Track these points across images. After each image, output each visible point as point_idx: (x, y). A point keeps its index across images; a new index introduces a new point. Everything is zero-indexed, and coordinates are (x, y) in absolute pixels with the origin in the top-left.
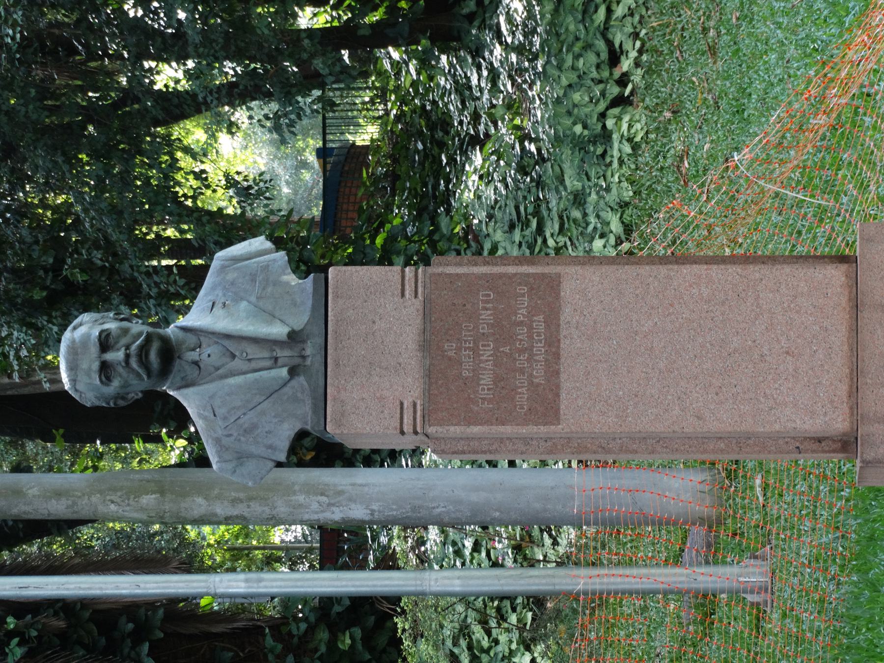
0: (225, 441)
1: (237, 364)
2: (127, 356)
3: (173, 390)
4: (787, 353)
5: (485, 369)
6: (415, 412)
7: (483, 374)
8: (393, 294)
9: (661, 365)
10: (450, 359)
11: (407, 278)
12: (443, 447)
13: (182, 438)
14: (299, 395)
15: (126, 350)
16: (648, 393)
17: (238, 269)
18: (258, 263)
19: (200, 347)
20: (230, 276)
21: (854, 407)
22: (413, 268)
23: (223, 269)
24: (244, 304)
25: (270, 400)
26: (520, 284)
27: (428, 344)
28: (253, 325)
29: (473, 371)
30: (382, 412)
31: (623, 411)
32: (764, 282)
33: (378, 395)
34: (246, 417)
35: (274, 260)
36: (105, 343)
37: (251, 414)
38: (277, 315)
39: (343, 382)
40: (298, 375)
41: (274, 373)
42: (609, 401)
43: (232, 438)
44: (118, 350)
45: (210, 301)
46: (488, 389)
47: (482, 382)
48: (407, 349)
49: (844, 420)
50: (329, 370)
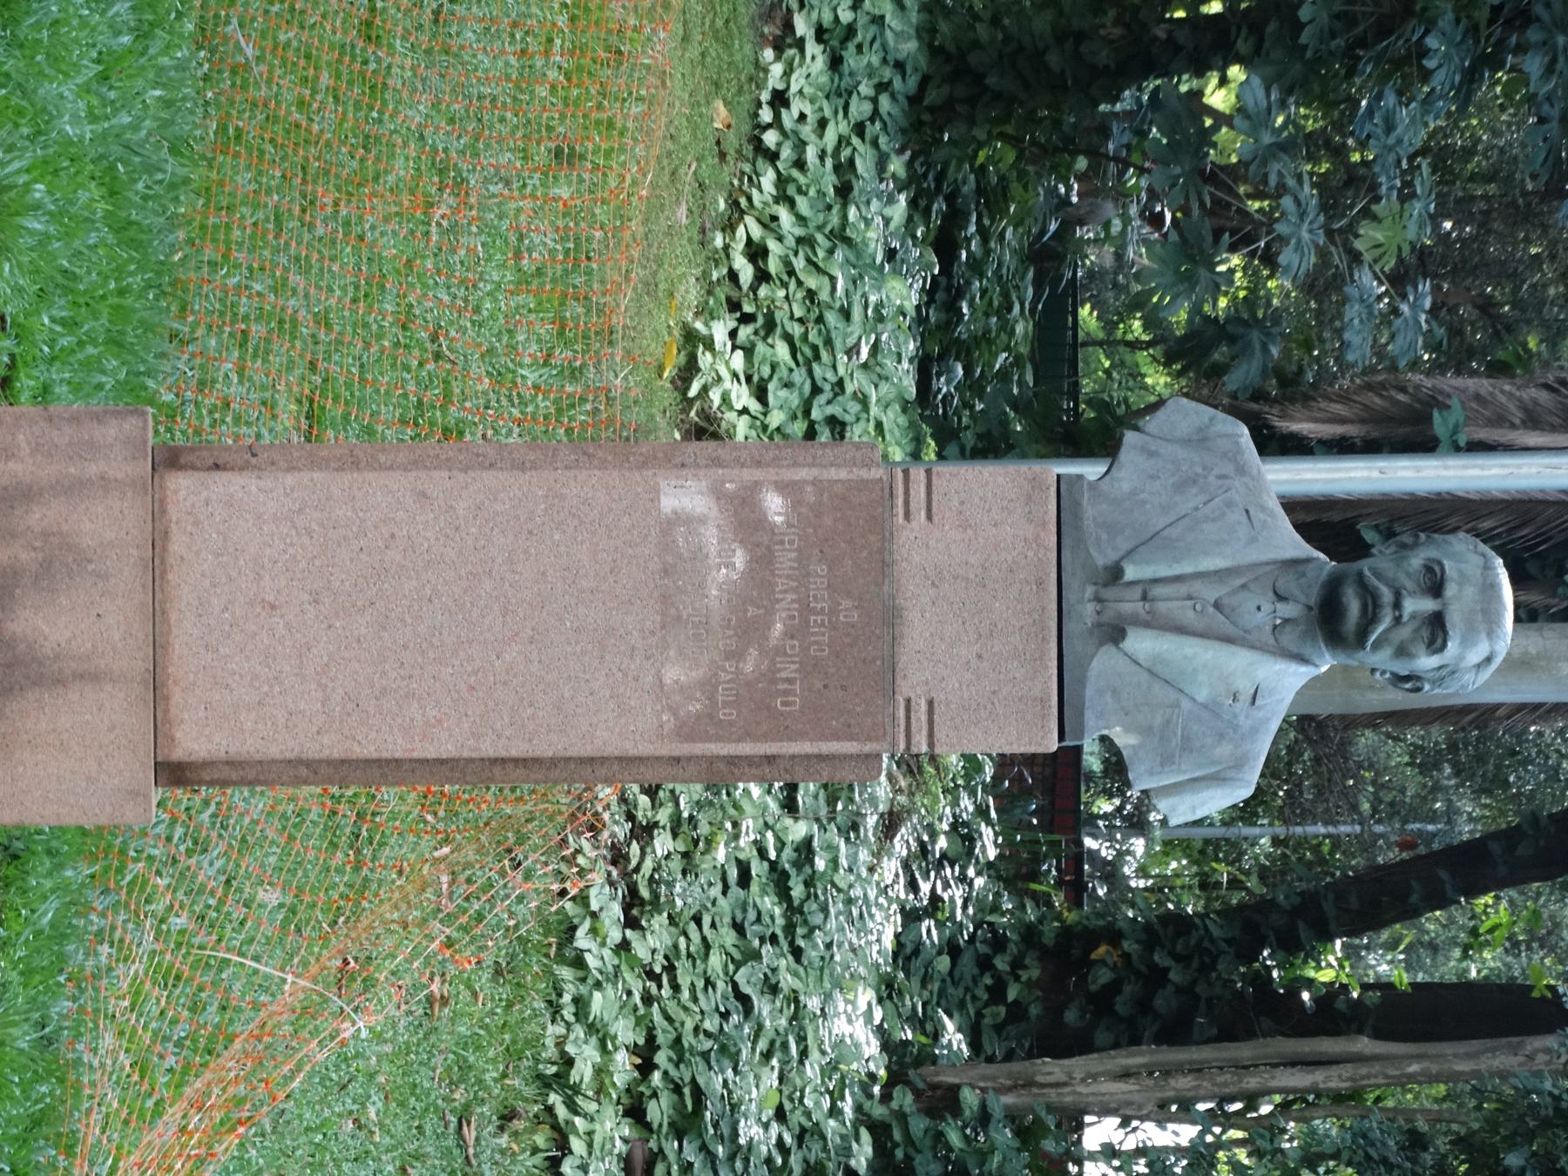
0: (1229, 469)
1: (1211, 592)
2: (1397, 605)
3: (1318, 559)
4: (273, 607)
5: (789, 577)
6: (907, 503)
7: (791, 568)
8: (948, 705)
9: (488, 585)
10: (849, 594)
11: (924, 732)
12: (858, 455)
13: (1324, 984)
14: (1104, 536)
15: (1401, 616)
16: (511, 537)
17: (1213, 763)
18: (1179, 772)
19: (1275, 627)
20: (1224, 750)
21: (158, 512)
22: (914, 750)
23: (1239, 764)
24: (1202, 695)
25: (1153, 530)
26: (731, 723)
27: (887, 619)
28: (1185, 657)
29: (808, 574)
30: (962, 503)
31: (552, 506)
32: (315, 729)
33: (970, 532)
34: (1191, 505)
35: (1151, 773)
36: (1436, 629)
37: (1185, 507)
38: (1145, 676)
39: (1030, 554)
40: (1106, 568)
41: (1148, 572)
42: (576, 522)
43: (1216, 471)
44: (1413, 616)
45: (1260, 708)
46: (782, 542)
47: (793, 555)
48: (923, 612)
49: (176, 492)
50: (1054, 576)
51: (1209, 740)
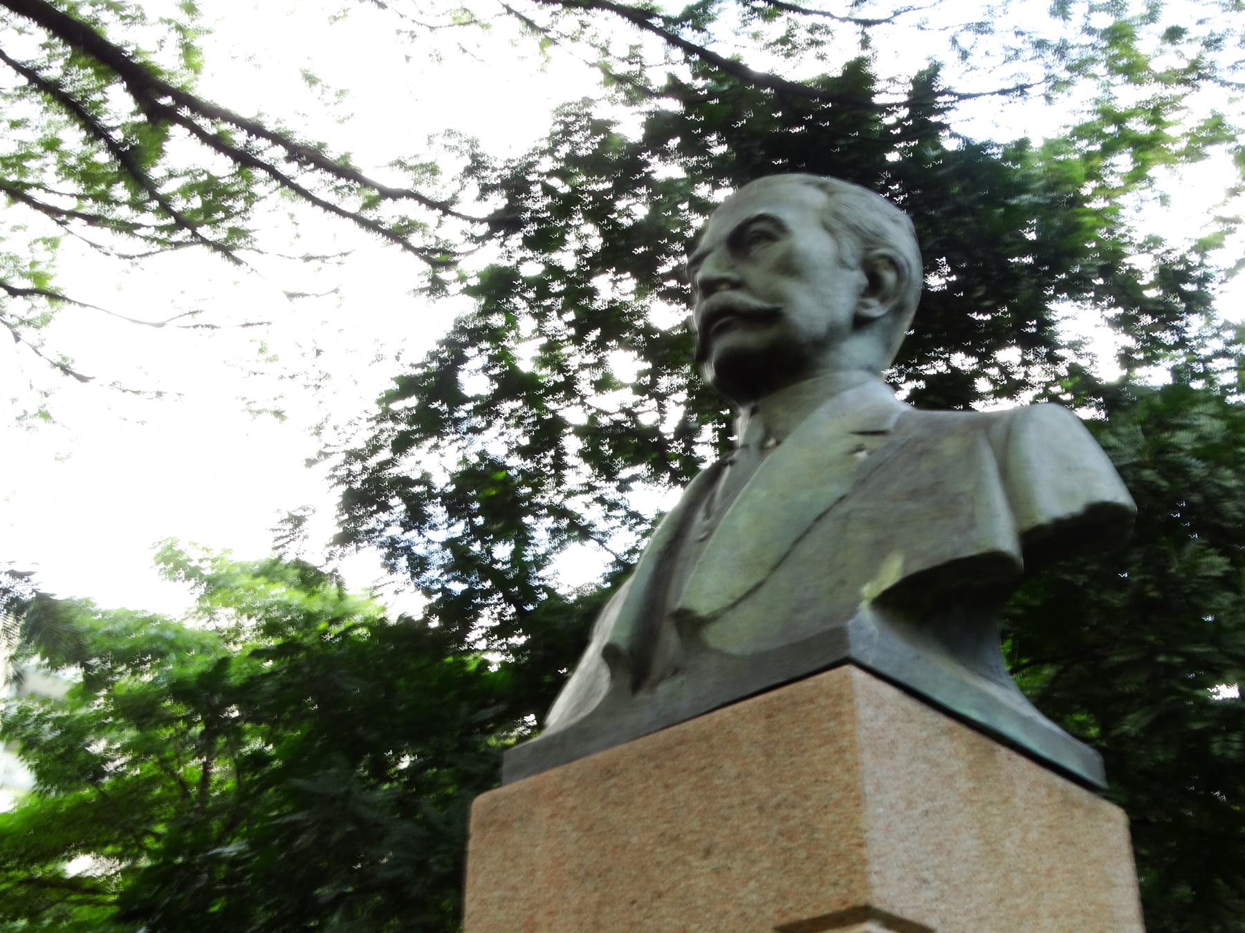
8: (782, 896)
39: (570, 802)
51: (926, 465)
